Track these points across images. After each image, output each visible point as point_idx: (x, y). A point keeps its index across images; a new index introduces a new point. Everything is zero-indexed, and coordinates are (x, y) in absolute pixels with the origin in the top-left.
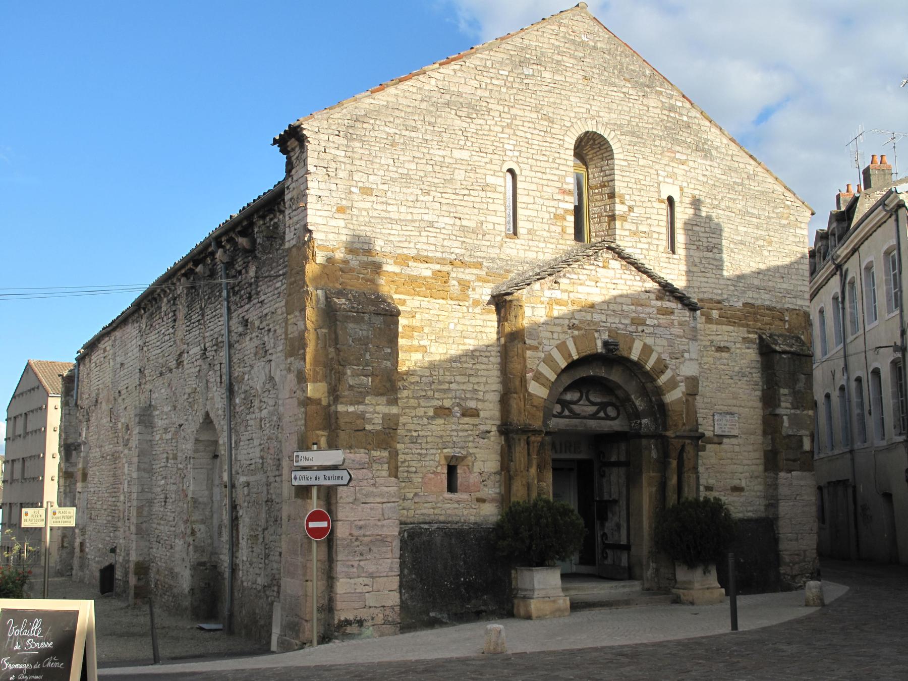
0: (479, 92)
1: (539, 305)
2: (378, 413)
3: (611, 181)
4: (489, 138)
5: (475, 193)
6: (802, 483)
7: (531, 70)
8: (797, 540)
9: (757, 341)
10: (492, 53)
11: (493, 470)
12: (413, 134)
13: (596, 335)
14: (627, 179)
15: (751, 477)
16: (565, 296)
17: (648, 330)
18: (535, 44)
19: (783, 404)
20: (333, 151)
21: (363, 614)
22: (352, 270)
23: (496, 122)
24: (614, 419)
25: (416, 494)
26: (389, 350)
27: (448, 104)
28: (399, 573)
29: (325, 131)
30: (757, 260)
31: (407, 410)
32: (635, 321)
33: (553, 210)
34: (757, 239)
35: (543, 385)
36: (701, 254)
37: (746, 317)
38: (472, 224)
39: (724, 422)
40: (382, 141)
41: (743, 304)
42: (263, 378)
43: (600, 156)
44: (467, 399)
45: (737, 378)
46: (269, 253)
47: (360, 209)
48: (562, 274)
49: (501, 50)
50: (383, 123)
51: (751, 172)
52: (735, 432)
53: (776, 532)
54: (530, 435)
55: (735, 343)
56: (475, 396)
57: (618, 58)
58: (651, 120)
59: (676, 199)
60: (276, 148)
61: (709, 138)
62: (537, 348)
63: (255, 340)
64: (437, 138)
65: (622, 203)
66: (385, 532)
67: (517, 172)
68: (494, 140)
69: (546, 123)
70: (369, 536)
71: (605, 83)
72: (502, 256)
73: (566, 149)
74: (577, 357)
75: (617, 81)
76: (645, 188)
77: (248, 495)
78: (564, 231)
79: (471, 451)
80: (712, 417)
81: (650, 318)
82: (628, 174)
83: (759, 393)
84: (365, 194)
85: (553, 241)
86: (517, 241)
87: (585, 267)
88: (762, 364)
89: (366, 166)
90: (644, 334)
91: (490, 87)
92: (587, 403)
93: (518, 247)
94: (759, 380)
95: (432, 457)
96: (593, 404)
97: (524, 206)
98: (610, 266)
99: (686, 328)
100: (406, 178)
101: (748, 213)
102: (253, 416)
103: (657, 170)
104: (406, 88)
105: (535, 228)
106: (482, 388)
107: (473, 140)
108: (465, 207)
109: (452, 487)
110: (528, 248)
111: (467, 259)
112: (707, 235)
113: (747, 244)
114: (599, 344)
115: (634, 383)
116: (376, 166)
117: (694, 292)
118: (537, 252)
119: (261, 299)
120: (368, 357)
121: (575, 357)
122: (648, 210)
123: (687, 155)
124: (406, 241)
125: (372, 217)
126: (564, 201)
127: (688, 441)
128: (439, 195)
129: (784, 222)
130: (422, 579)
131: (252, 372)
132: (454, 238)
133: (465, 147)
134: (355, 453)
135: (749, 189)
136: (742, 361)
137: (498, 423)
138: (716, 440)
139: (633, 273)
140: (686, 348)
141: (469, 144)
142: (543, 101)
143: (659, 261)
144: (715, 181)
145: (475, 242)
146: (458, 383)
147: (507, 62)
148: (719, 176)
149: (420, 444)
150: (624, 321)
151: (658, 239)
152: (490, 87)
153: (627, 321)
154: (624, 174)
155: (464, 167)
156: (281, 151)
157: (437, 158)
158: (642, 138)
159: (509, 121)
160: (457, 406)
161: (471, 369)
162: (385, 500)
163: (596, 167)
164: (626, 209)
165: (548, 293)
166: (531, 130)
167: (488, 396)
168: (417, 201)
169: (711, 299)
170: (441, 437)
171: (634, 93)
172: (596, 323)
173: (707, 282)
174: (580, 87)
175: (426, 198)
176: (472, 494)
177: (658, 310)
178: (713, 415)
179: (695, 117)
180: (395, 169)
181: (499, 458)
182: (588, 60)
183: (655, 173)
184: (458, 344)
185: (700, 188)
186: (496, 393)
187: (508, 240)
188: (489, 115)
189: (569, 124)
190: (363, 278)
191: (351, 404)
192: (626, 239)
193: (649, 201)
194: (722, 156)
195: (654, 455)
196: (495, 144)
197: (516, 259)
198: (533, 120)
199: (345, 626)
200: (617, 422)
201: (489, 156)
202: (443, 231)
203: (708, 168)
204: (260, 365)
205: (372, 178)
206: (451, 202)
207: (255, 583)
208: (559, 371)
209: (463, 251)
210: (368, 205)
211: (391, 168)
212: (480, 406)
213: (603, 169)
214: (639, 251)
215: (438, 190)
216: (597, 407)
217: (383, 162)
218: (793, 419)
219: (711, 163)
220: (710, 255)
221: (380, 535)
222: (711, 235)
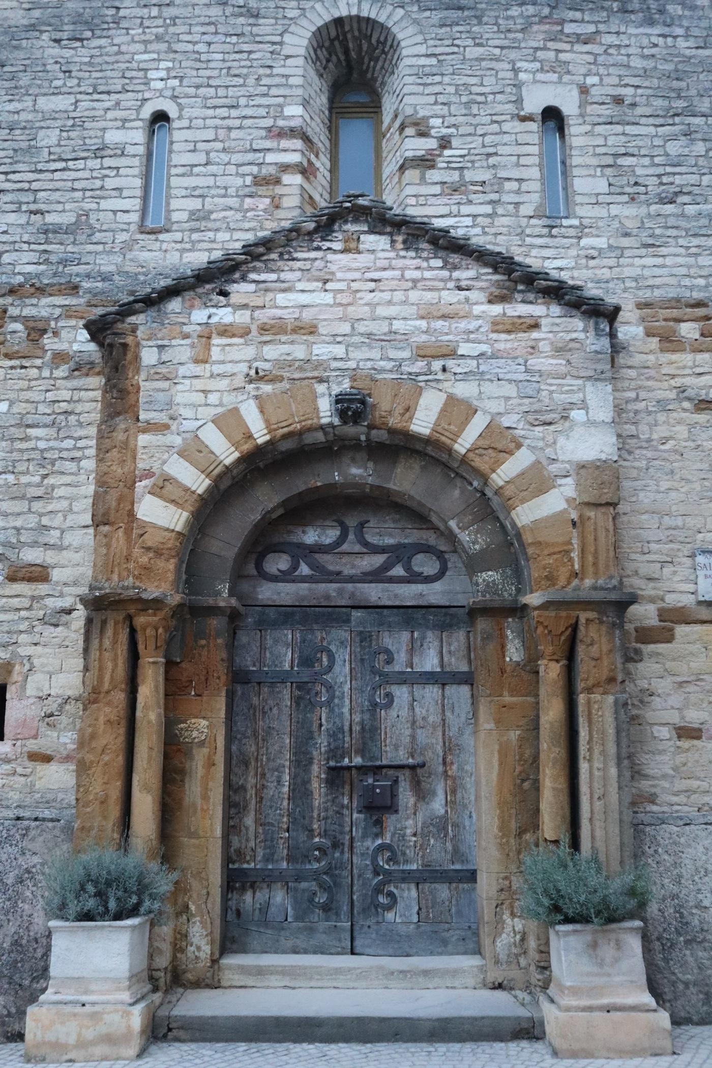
4: (116, 66)
5: (80, 164)
11: (70, 693)
14: (438, 89)
16: (242, 318)
23: (133, 36)
24: (429, 580)
27: (32, 27)
32: (422, 353)
33: (255, 169)
36: (643, 210)
38: (68, 218)
48: (237, 275)
54: (132, 611)
56: (42, 540)
59: (569, 106)
62: (167, 427)
65: (423, 134)
67: (173, 113)
69: (242, 20)
72: (127, 269)
73: (288, 57)
74: (268, 437)
76: (480, 99)
79: (23, 651)
81: (468, 341)
82: (437, 79)
85: (247, 225)
87: (295, 255)
90: (448, 375)
92: (358, 548)
93: (164, 246)
96: (381, 550)
98: (361, 247)
99: (576, 358)
103: (513, 62)
106: (57, 521)
107: (81, 74)
110: (188, 246)
111: (46, 281)
112: (660, 170)
115: (457, 493)
118: (210, 250)
127: (583, 616)
132: (25, 247)
139: (425, 254)
140: (576, 398)
145: (70, 248)
148: (688, 52)
150: (392, 354)
151: (518, 192)
154: (429, 81)
155: (58, 123)
159: (161, 30)
161: (39, 485)
165: (199, 315)
166: (207, 38)
167: (69, 539)
169: (678, 300)
172: (319, 365)
173: (663, 266)
177: (495, 324)
178: (693, 556)
183: (510, 67)
184: (13, 440)
185: (636, 81)
195: (514, 653)
197: (159, 270)
198: (213, 19)
200: (437, 586)
201: (118, 96)
206: (26, 186)
209: (42, 267)
212: (49, 557)
214: (468, 221)
216: (386, 556)
220: (669, 209)
222: (669, 169)
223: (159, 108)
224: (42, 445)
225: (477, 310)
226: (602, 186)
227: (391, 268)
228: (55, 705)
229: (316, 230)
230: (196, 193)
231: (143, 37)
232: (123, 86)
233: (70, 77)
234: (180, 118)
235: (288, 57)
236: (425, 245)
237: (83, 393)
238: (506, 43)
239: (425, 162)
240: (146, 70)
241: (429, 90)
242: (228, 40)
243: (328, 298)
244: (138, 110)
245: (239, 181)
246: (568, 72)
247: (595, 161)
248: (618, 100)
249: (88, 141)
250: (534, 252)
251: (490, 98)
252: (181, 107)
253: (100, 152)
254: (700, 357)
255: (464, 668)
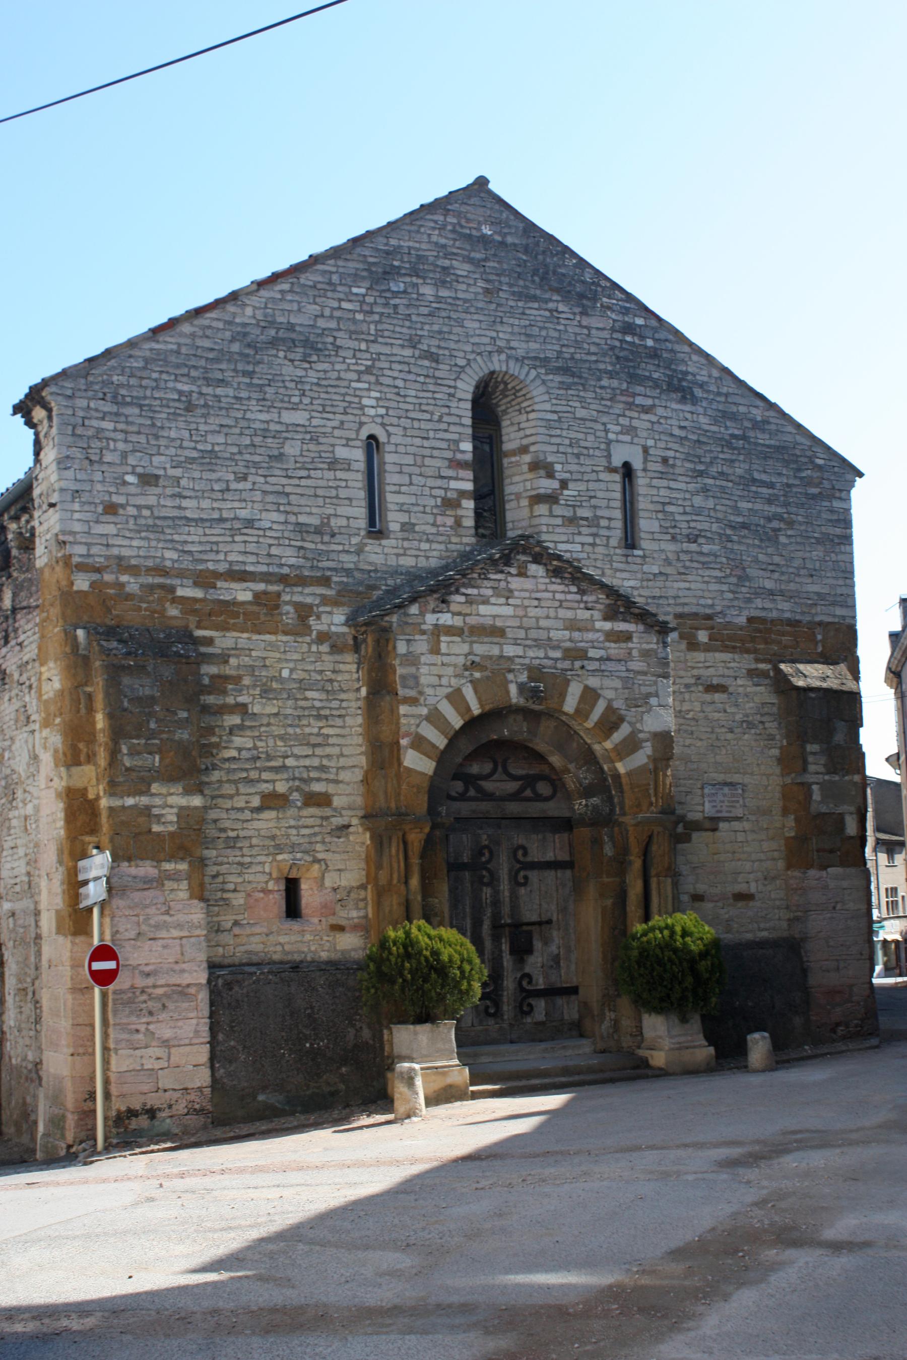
0: (321, 323)
1: (417, 637)
2: (171, 807)
3: (533, 444)
5: (319, 474)
6: (845, 884)
7: (402, 285)
8: (838, 969)
9: (772, 674)
10: (340, 263)
11: (354, 884)
12: (219, 391)
13: (510, 677)
15: (765, 879)
16: (458, 621)
17: (593, 666)
18: (406, 244)
19: (812, 768)
20: (95, 423)
21: (153, 1100)
22: (129, 597)
23: (349, 364)
24: (547, 799)
25: (236, 923)
26: (184, 715)
28: (208, 1039)
29: (84, 394)
30: (770, 550)
31: (220, 800)
33: (441, 493)
34: (769, 519)
35: (425, 754)
37: (753, 639)
38: (315, 521)
39: (720, 797)
40: (172, 404)
41: (750, 620)
42: (25, 757)
43: (517, 407)
44: (312, 779)
45: (739, 730)
46: (27, 571)
47: (139, 507)
48: (453, 589)
49: (355, 256)
50: (173, 377)
51: (759, 418)
52: (739, 812)
53: (805, 959)
55: (736, 678)
56: (324, 776)
57: (540, 257)
58: (593, 349)
59: (637, 464)
60: (19, 419)
61: (690, 369)
63: (14, 700)
64: (255, 395)
65: (550, 475)
66: (186, 979)
67: (382, 438)
68: (346, 394)
69: (426, 363)
70: (162, 986)
71: (519, 296)
73: (460, 400)
75: (538, 292)
76: (585, 452)
77: (14, 930)
78: (458, 523)
79: (320, 856)
80: (699, 792)
81: (594, 647)
82: (558, 432)
83: (776, 752)
84: (148, 483)
86: (384, 542)
88: (779, 709)
89: (148, 443)
91: (337, 314)
92: (505, 777)
93: (386, 550)
94: (774, 732)
95: (259, 868)
96: (515, 778)
97: (393, 488)
98: (529, 573)
100: (209, 459)
101: (754, 480)
102: (16, 813)
103: (604, 424)
104: (206, 322)
105: (413, 521)
108: (302, 495)
109: (293, 910)
110: (401, 551)
111: (307, 573)
112: (688, 518)
113: (753, 527)
114: (513, 689)
116: (162, 442)
117: (669, 605)
119: (20, 640)
120: (153, 725)
121: (476, 710)
122: (592, 485)
123: (653, 398)
124: (212, 551)
125: (159, 518)
126: (456, 479)
128: (262, 480)
129: (814, 491)
130: (244, 1047)
131: (13, 748)
132: (287, 542)
133: (301, 406)
134: (137, 866)
135: (756, 444)
136: (748, 706)
137: (361, 813)
138: (707, 824)
139: (566, 582)
140: (652, 690)
141: (306, 401)
142: (422, 329)
143: (611, 561)
144: (699, 435)
145: (320, 546)
146: (297, 757)
147: (365, 274)
148: (707, 427)
149: (241, 848)
151: (608, 528)
152: (337, 314)
153: (558, 654)
155: (299, 436)
156: (27, 423)
157: (257, 425)
158: (580, 377)
159: (369, 363)
160: (297, 790)
161: (318, 735)
162: (186, 934)
163: (512, 424)
164: (555, 484)
165: (430, 618)
166: (402, 375)
167: (344, 776)
168: (228, 490)
170: (273, 838)
171: (566, 309)
172: (510, 659)
173: (689, 589)
174: (480, 305)
175: (241, 486)
176: (323, 919)
178: (702, 788)
179: (666, 340)
180: (193, 445)
181: (363, 865)
182: (492, 264)
183: (602, 428)
184: (296, 699)
185: (676, 446)
186: (357, 770)
187: (370, 541)
188: (337, 355)
189: (462, 362)
190: (146, 610)
191: (129, 796)
192: (558, 530)
193: (593, 471)
194: (711, 397)
196: (348, 398)
197: (384, 569)
198: (406, 360)
199: (128, 1118)
200: (551, 804)
201: (338, 417)
202: (268, 533)
203: (689, 416)
204: (22, 736)
205: (156, 460)
206: (280, 489)
207: (25, 1059)
208: (452, 733)
210: (152, 500)
211: (186, 444)
212: (331, 788)
213: (522, 426)
215: (260, 472)
217: (173, 434)
218: (828, 790)
219: (692, 408)
220: (693, 547)
221: (179, 985)
222: (694, 518)
223: (373, 432)
224: (318, 704)
225: (599, 625)
226: (655, 526)
227: (546, 591)
228: (345, 893)
229: (500, 558)
230: (405, 507)
231: (356, 368)
232: (345, 408)
233: (304, 395)
234: (389, 442)
235: (460, 400)
236: (567, 575)
237: (341, 665)
238: (601, 408)
239: (551, 499)
240: (361, 397)
241: (554, 440)
242: (418, 379)
243: (508, 611)
244: (358, 431)
245: (432, 502)
246: (637, 436)
247: (651, 507)
248: (665, 460)
249: (323, 455)
250: (618, 574)
251: (591, 451)
252: (389, 435)
253: (334, 464)
254: (709, 655)
255: (567, 858)
